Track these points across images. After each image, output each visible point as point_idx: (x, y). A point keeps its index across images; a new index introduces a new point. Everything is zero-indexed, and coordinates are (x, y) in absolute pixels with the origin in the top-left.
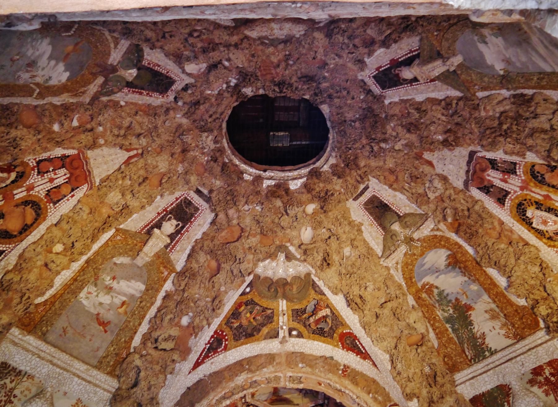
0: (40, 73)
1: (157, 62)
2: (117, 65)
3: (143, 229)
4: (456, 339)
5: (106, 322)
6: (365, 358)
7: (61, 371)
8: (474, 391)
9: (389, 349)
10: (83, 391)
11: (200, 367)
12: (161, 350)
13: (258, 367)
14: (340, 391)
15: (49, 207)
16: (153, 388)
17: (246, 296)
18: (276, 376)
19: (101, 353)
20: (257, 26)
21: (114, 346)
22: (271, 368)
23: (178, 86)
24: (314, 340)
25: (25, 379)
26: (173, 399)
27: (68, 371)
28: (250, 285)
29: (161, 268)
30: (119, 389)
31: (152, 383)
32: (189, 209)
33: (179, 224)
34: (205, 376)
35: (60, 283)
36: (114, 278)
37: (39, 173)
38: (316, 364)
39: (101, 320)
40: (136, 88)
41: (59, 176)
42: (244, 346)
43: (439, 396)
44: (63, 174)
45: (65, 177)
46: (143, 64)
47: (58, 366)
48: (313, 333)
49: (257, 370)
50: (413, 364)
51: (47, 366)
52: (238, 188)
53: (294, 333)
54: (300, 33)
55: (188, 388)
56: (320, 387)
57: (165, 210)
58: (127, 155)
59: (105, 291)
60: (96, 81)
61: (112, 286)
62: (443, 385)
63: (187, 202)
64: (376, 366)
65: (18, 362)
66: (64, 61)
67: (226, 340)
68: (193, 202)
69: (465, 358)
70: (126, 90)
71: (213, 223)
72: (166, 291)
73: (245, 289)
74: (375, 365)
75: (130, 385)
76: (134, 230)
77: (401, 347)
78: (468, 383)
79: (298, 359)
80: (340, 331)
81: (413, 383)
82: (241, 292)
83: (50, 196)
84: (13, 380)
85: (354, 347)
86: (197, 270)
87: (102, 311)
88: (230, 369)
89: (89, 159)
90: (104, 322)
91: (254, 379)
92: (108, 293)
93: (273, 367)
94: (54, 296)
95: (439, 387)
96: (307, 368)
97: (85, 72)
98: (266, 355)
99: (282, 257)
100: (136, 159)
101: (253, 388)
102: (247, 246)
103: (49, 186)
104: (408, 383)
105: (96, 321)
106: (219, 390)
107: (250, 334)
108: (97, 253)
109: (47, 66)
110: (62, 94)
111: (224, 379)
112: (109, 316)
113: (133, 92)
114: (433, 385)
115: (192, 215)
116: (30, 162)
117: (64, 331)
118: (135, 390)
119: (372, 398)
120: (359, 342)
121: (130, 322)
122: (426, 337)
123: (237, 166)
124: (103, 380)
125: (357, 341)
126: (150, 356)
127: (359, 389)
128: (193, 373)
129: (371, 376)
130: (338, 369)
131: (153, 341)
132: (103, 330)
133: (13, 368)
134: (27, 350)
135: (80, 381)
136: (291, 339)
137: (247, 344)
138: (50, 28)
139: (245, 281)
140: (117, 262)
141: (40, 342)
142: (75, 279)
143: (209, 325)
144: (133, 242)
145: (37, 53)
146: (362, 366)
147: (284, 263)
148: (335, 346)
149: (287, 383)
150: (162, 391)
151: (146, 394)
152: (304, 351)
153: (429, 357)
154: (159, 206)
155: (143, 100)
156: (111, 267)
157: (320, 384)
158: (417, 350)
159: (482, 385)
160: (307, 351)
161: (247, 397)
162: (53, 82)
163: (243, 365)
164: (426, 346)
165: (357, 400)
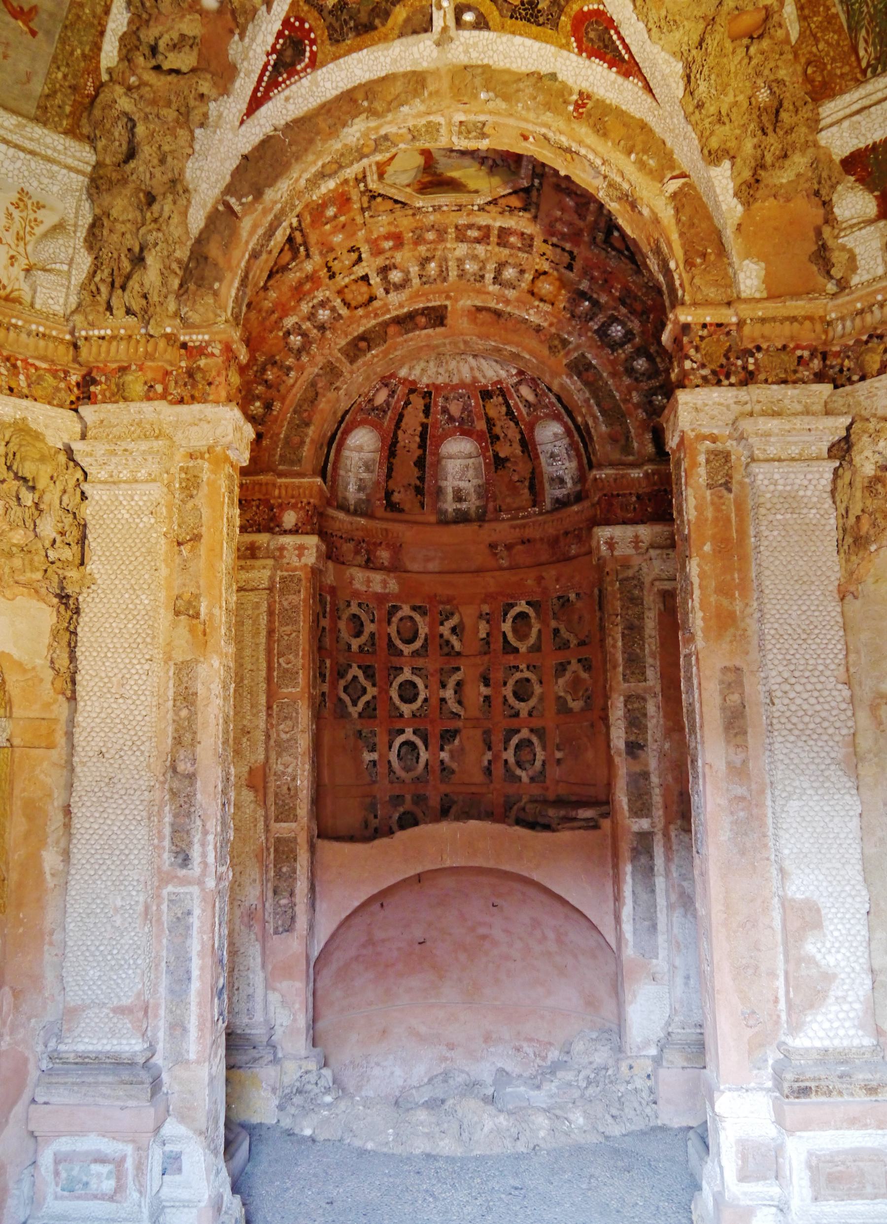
4: (843, 18)
5: (26, 9)
6: (627, 75)
8: (855, 141)
9: (685, 48)
11: (263, 110)
12: (171, 71)
13: (390, 103)
14: (568, 150)
16: (169, 159)
18: (429, 122)
19: (38, 87)
21: (63, 69)
22: (418, 106)
24: (513, 33)
26: (217, 181)
30: (98, 165)
31: (166, 148)
34: (275, 130)
38: (518, 91)
42: (354, 55)
43: (777, 153)
48: (512, 17)
49: (389, 111)
50: (734, 84)
53: (469, 17)
55: (245, 157)
56: (524, 144)
62: (792, 129)
64: (651, 91)
67: (313, 42)
69: (855, 64)
74: (648, 89)
75: (121, 157)
77: (711, 44)
78: (846, 124)
79: (478, 81)
80: (576, 7)
81: (727, 127)
85: (606, 47)
88: (329, 111)
90: (22, 9)
91: (382, 132)
93: (423, 101)
95: (781, 133)
96: (499, 101)
98: (405, 75)
101: (381, 152)
104: (717, 127)
106: (311, 158)
107: (365, 26)
111: (318, 133)
114: (770, 131)
118: (132, 164)
119: (634, 163)
120: (618, 33)
122: (776, 16)
125: (612, 32)
126: (148, 89)
127: (610, 144)
128: (249, 122)
129: (638, 116)
130: (566, 102)
131: (147, 52)
132: (25, 29)
136: (460, 32)
137: (361, 49)
146: (621, 92)
148: (562, 47)
149: (455, 139)
150: (189, 164)
151: (157, 172)
152: (491, 63)
153: (772, 64)
157: (526, 138)
158: (748, 48)
159: (876, 126)
160: (498, 61)
161: (369, 179)
163: (356, 101)
164: (772, 38)
165: (603, 169)
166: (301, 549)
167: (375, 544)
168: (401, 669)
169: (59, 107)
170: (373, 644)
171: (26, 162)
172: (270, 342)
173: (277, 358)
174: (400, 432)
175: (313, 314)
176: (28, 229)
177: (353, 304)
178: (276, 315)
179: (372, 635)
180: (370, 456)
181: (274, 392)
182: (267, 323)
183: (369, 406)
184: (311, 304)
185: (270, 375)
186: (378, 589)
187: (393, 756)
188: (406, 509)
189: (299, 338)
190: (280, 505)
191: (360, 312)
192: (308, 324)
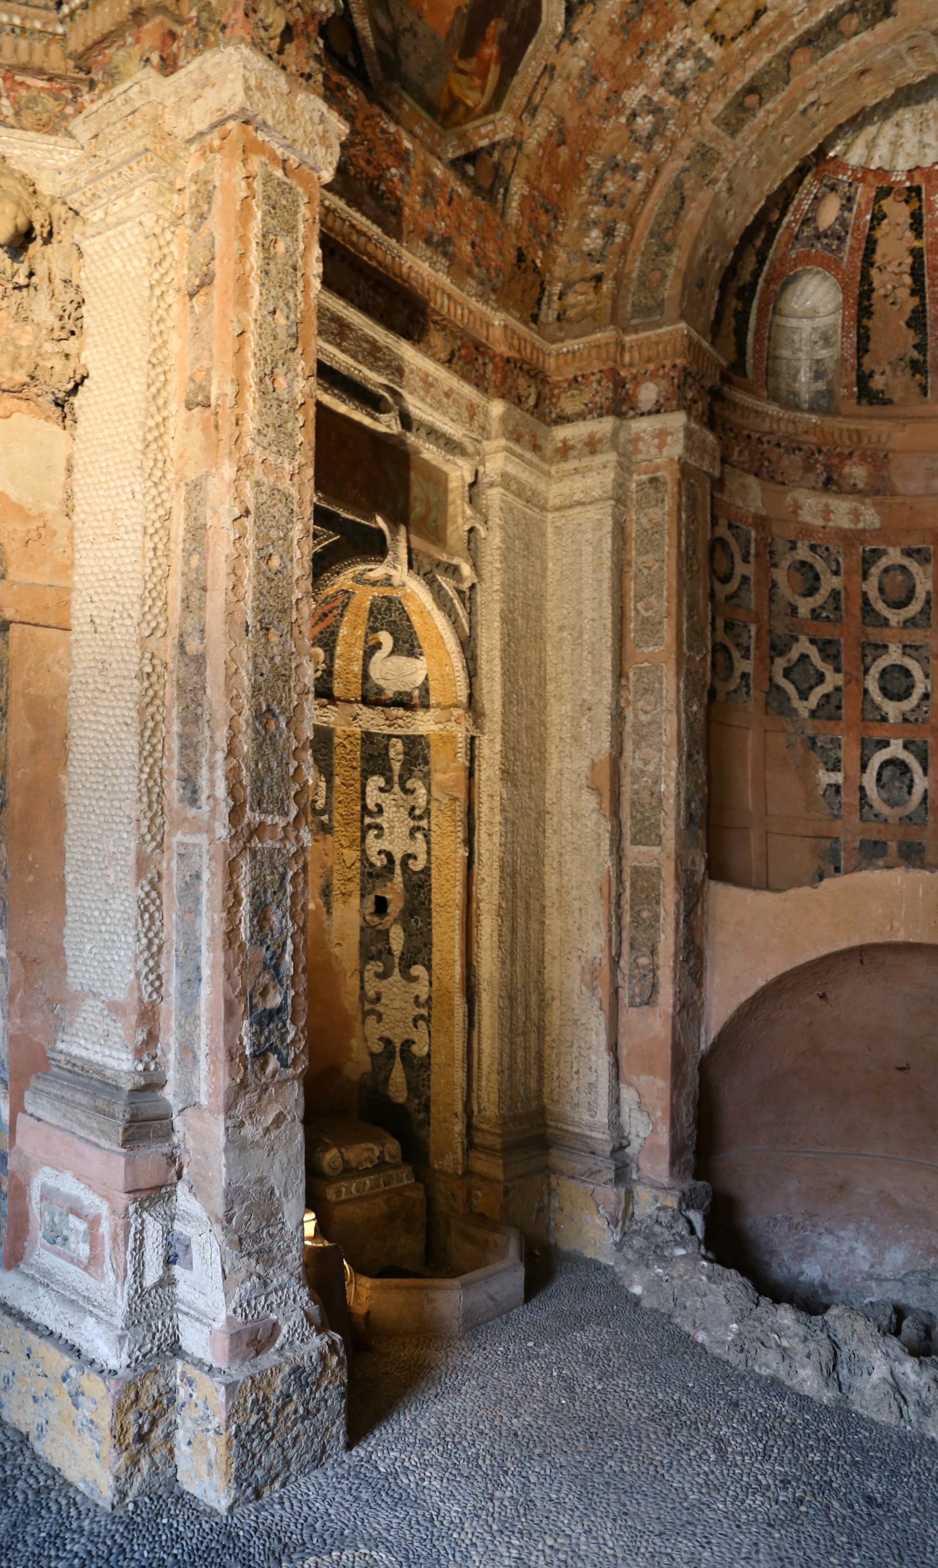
166: (662, 434)
167: (839, 455)
168: (886, 647)
170: (837, 608)
172: (609, 138)
173: (619, 157)
174: (874, 272)
175: (667, 74)
177: (729, 35)
178: (603, 87)
179: (835, 594)
180: (828, 320)
181: (616, 208)
182: (591, 101)
183: (808, 231)
184: (664, 59)
185: (610, 188)
186: (846, 523)
187: (869, 780)
188: (896, 398)
189: (650, 118)
190: (635, 377)
191: (741, 43)
192: (661, 91)
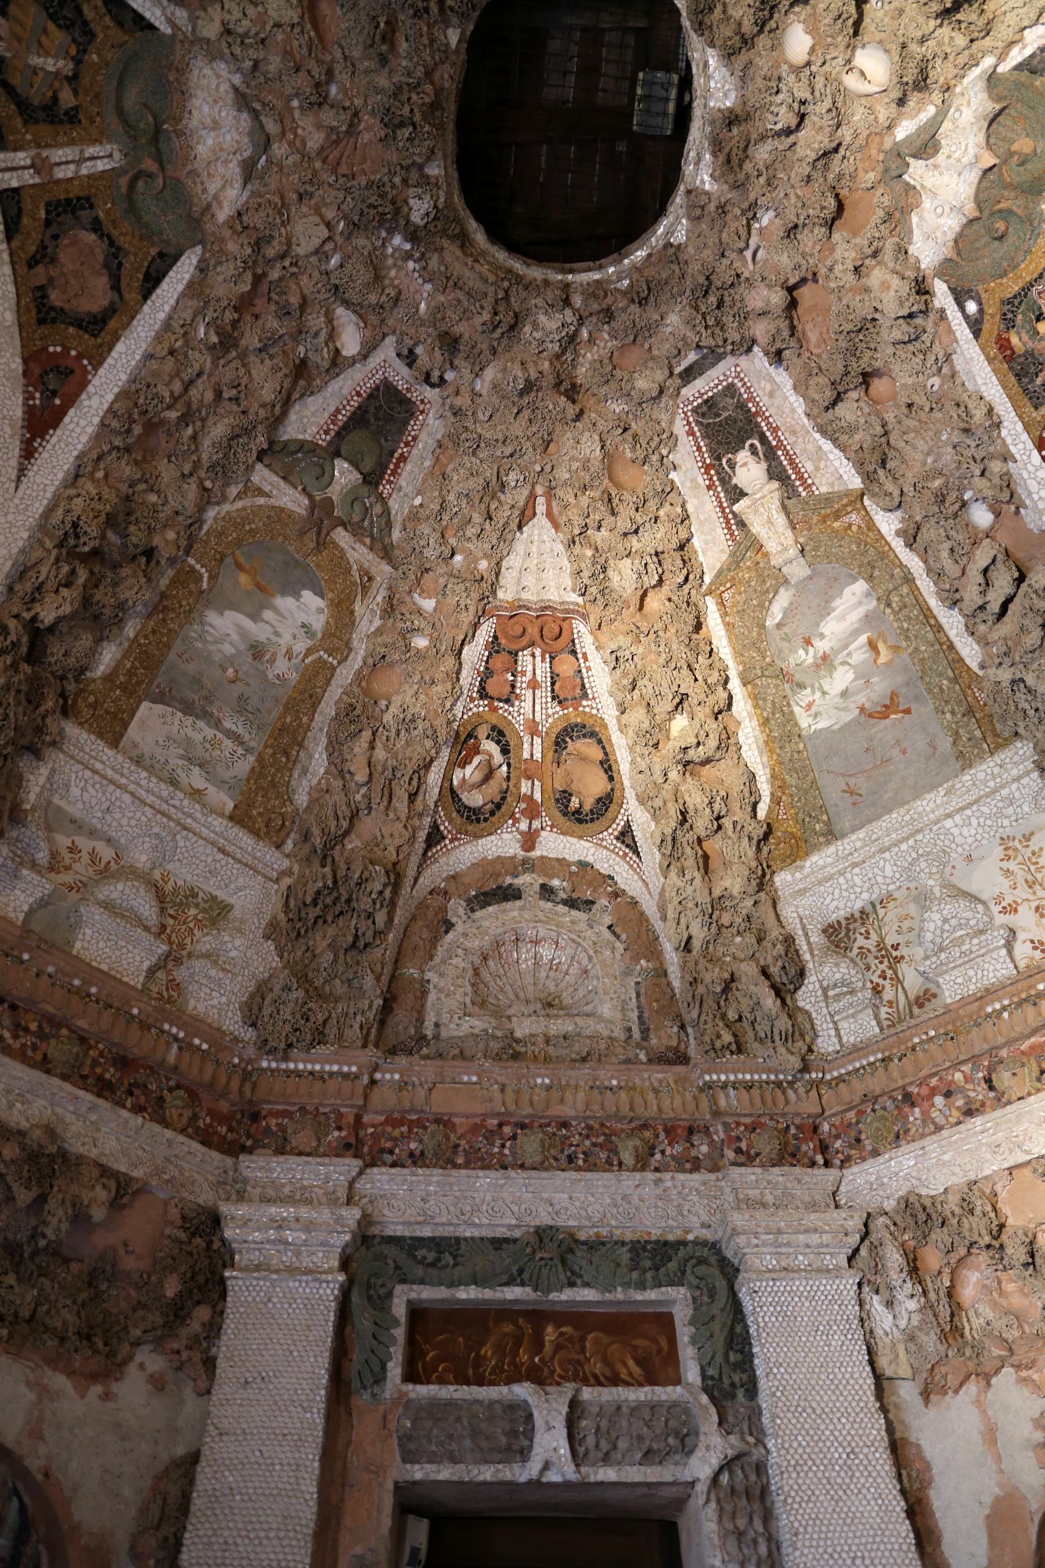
0: (286, 640)
1: (326, 415)
2: (310, 497)
3: (732, 535)
7: (911, 842)
10: (989, 822)
15: (587, 710)
17: (987, 317)
19: (945, 743)
20: (205, 190)
23: (401, 376)
25: (881, 912)
27: (919, 831)
28: (960, 297)
29: (836, 525)
32: (725, 409)
33: (752, 445)
35: (756, 753)
36: (808, 642)
37: (507, 701)
39: (879, 709)
40: (387, 467)
41: (530, 668)
44: (530, 658)
45: (539, 659)
46: (324, 444)
47: (897, 843)
51: (882, 863)
52: (694, 267)
54: (224, 73)
57: (707, 468)
58: (541, 520)
59: (823, 672)
60: (342, 544)
61: (821, 653)
63: (705, 409)
65: (841, 905)
66: (273, 595)
68: (710, 394)
70: (385, 489)
71: (777, 357)
72: (898, 533)
73: (966, 317)
76: (724, 557)
82: (967, 331)
83: (566, 699)
84: (867, 932)
86: (868, 438)
87: (861, 699)
89: (519, 600)
90: (885, 706)
92: (832, 668)
94: (773, 777)
97: (311, 561)
99: (917, 171)
100: (554, 504)
102: (850, 277)
103: (544, 694)
105: (872, 721)
108: (738, 654)
109: (273, 626)
110: (352, 613)
112: (880, 687)
113: (394, 473)
115: (742, 406)
116: (475, 710)
117: (851, 793)
121: (917, 650)
123: (650, 255)
124: (996, 770)
132: (900, 715)
133: (847, 919)
134: (831, 877)
135: (957, 818)
138: (181, 606)
139: (942, 311)
140: (777, 620)
141: (832, 849)
142: (765, 722)
143: (1007, 457)
144: (749, 568)
145: (235, 637)
147: (936, 167)
154: (694, 480)
155: (422, 458)
156: (782, 639)
162: (318, 623)
169: (970, 739)
171: (977, 814)
176: (1033, 868)
